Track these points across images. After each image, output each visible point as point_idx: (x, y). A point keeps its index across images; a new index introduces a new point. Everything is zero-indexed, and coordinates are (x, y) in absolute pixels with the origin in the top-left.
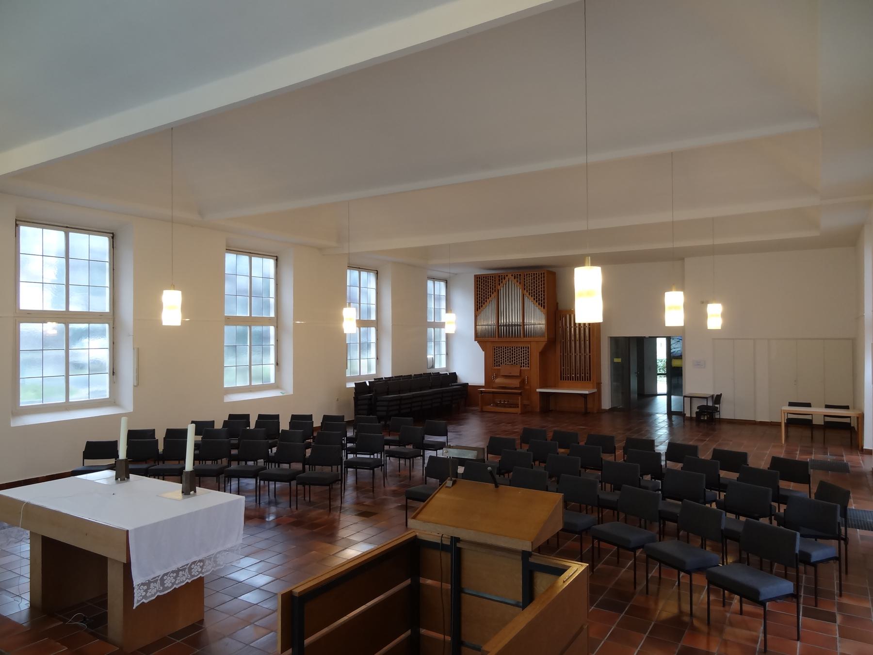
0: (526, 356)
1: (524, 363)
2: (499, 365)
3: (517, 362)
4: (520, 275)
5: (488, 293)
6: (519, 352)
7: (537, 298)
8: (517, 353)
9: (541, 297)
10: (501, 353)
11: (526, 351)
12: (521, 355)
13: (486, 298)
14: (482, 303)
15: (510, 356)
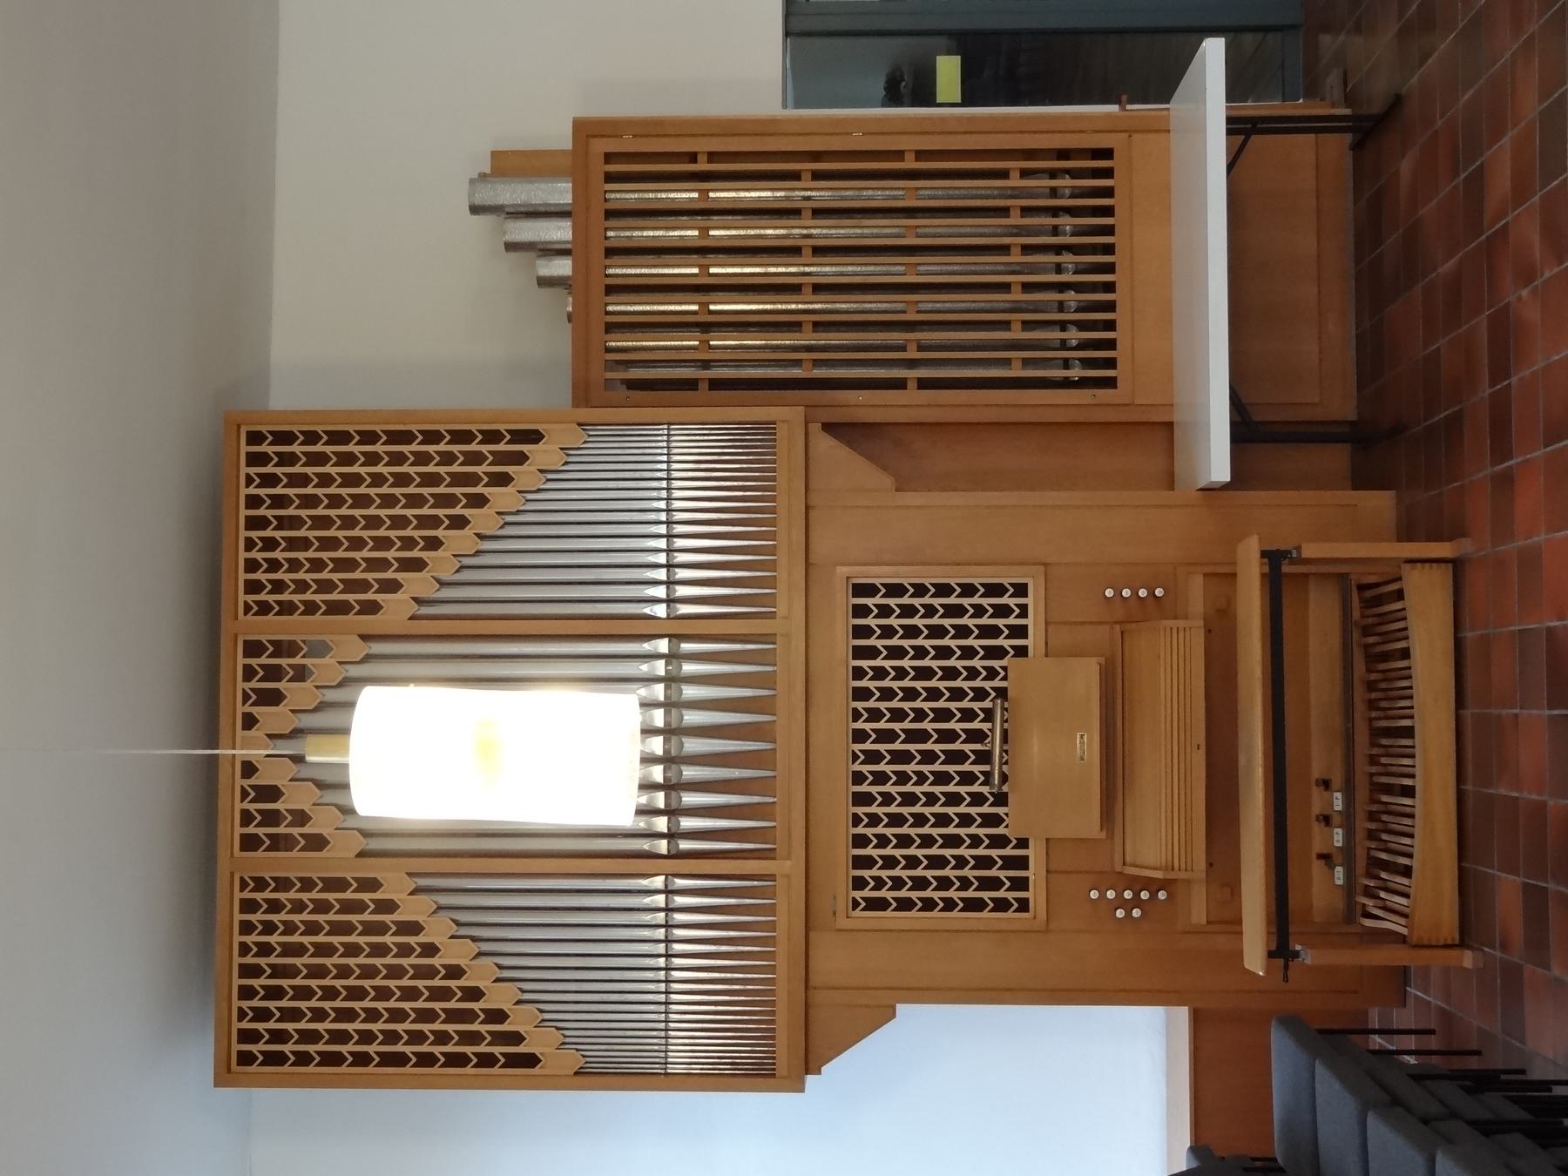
0: (930, 611)
1: (993, 632)
2: (1009, 863)
3: (980, 694)
4: (253, 649)
5: (379, 950)
6: (901, 673)
7: (449, 501)
8: (911, 694)
9: (448, 459)
10: (905, 841)
11: (885, 611)
12: (921, 653)
13: (430, 972)
14: (469, 1016)
15: (929, 757)
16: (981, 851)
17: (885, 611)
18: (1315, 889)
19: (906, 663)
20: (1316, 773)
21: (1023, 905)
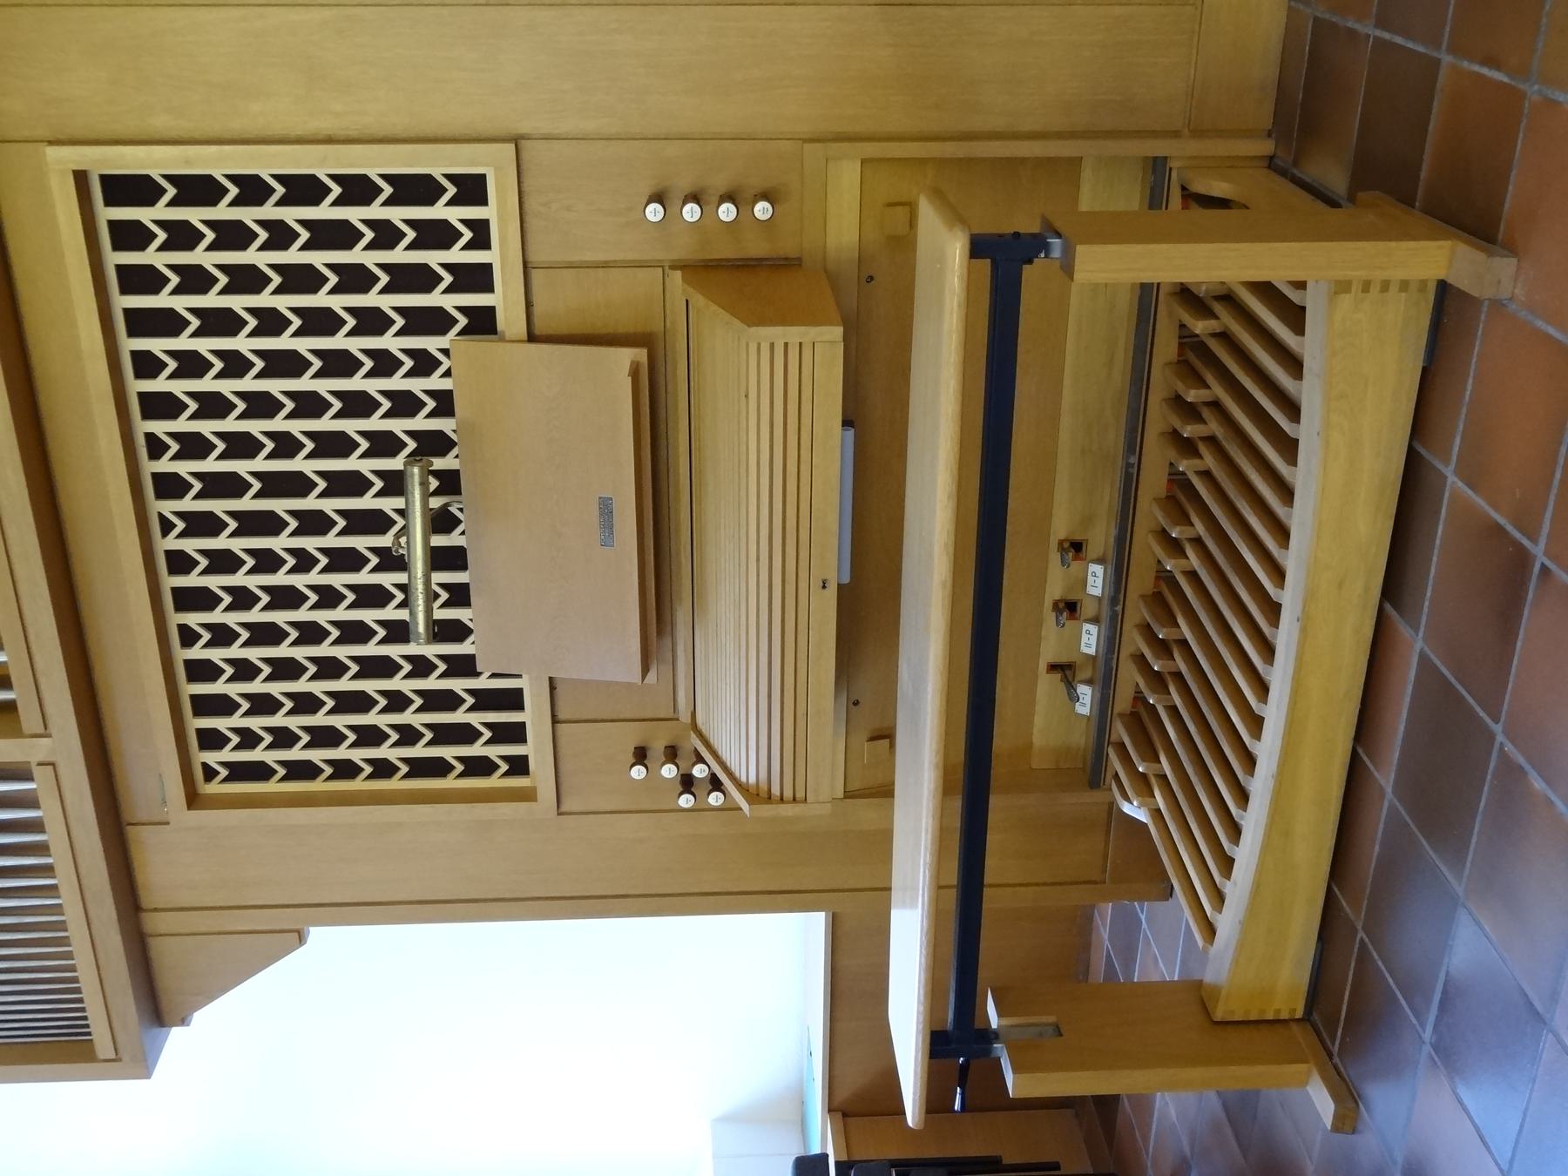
1: (420, 278)
3: (404, 404)
8: (261, 405)
12: (270, 322)
15: (314, 523)
16: (432, 683)
17: (182, 236)
18: (1039, 721)
19: (242, 343)
20: (1061, 528)
21: (519, 766)
